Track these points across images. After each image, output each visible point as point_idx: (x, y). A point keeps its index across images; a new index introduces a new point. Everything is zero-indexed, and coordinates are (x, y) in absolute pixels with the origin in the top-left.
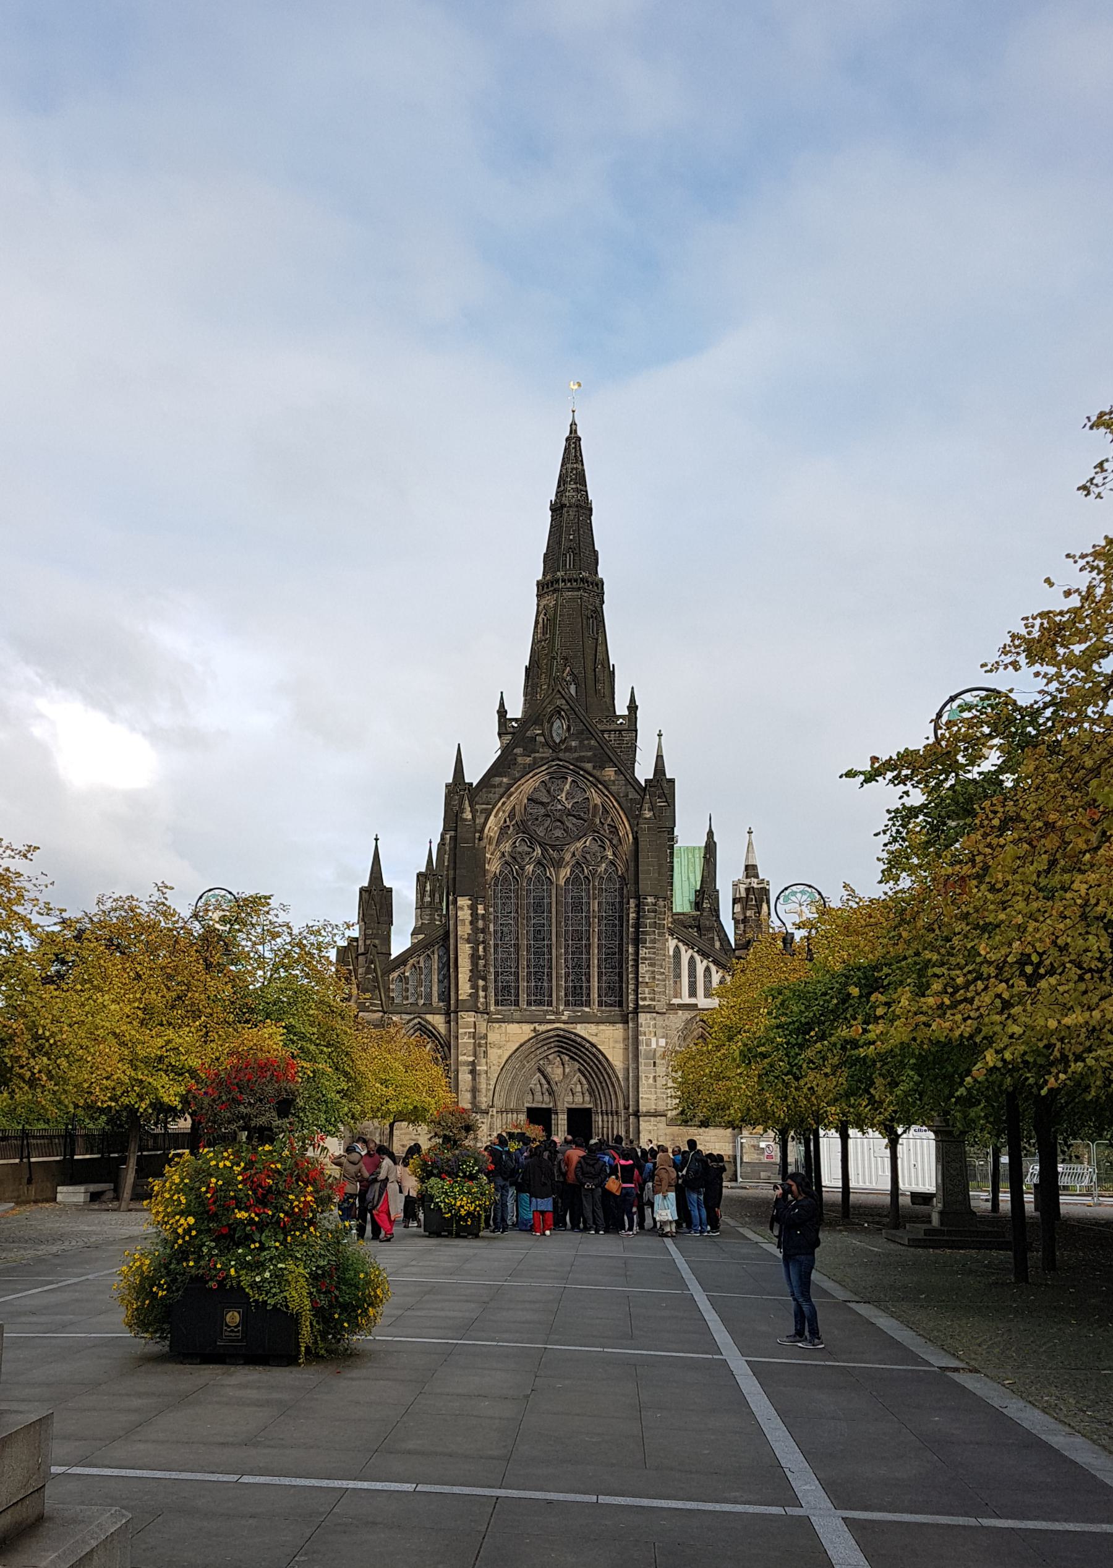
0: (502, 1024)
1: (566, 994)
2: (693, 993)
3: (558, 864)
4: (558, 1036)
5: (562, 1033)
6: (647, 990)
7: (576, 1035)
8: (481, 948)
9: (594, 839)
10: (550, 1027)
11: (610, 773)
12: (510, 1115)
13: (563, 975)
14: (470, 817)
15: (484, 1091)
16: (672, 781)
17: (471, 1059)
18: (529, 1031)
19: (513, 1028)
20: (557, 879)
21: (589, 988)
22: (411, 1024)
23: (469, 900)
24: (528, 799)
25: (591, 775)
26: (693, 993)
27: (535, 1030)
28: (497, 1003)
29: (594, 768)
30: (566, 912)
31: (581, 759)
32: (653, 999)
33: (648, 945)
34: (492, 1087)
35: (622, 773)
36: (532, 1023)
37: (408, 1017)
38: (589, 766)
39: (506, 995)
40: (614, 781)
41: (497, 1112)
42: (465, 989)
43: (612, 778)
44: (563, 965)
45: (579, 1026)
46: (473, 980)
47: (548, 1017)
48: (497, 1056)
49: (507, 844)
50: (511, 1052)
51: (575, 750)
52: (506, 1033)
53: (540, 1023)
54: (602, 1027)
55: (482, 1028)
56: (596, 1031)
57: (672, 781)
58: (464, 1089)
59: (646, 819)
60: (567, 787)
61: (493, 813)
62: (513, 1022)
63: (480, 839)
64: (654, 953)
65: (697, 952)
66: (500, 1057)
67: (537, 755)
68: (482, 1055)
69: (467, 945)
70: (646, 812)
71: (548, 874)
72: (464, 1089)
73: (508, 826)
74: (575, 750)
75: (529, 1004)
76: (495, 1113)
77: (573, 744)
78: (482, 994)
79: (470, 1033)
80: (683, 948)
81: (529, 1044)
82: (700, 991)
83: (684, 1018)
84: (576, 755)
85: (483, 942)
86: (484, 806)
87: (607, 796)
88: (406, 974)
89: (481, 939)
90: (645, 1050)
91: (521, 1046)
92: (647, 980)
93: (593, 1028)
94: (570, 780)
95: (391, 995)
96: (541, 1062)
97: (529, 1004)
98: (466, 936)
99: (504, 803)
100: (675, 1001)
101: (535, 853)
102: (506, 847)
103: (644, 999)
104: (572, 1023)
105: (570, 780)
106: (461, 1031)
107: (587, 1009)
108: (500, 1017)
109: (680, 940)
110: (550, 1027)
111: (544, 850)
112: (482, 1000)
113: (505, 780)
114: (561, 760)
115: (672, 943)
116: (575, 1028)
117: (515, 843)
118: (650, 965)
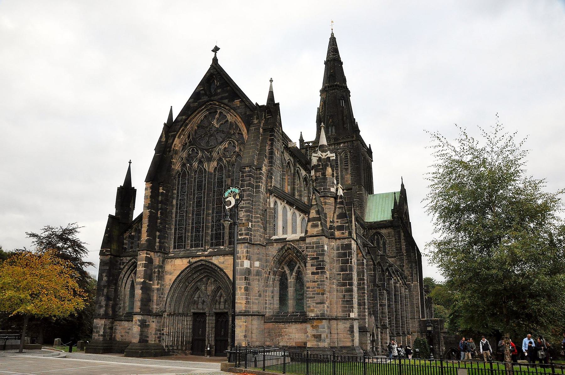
0: (173, 260)
1: (211, 238)
2: (285, 231)
3: (209, 160)
4: (202, 264)
5: (203, 263)
6: (243, 228)
7: (212, 263)
8: (159, 213)
9: (230, 143)
10: (197, 259)
11: (237, 102)
12: (177, 317)
13: (210, 227)
14: (164, 140)
15: (155, 301)
16: (278, 104)
17: (142, 280)
18: (186, 263)
19: (178, 262)
20: (209, 168)
21: (224, 233)
22: (130, 263)
23: (151, 183)
24: (198, 127)
25: (227, 105)
26: (285, 231)
27: (189, 262)
28: (174, 248)
29: (229, 101)
30: (214, 188)
31: (222, 98)
32: (247, 234)
33: (245, 198)
34: (165, 299)
35: (243, 101)
36: (188, 257)
37: (129, 258)
38: (226, 101)
39: (180, 243)
40: (239, 107)
41: (167, 315)
42: (144, 237)
43: (238, 105)
44: (210, 221)
45: (214, 258)
46: (151, 232)
47: (198, 253)
48: (169, 279)
49: (185, 153)
50: (176, 276)
51: (219, 94)
52: (174, 265)
53: (193, 257)
54: (227, 257)
55: (157, 261)
56: (223, 260)
57: (278, 104)
58: (137, 300)
59: (255, 124)
60: (217, 116)
61: (177, 137)
62: (178, 258)
63: (170, 151)
64: (249, 203)
65: (287, 203)
66: (170, 280)
67: (200, 101)
68: (155, 279)
69: (148, 210)
70: (255, 120)
71: (205, 166)
72: (137, 300)
73: (186, 144)
74: (219, 94)
75: (191, 247)
76: (166, 316)
77: (219, 91)
78: (158, 240)
79: (143, 264)
80: (279, 202)
81: (186, 271)
82: (289, 229)
83: (277, 248)
84: (219, 97)
85: (161, 209)
86: (173, 133)
87: (235, 116)
88: (132, 234)
89: (160, 207)
90: (240, 269)
91: (182, 272)
92: (244, 222)
93: (221, 259)
94: (218, 112)
95: (125, 246)
96: (199, 284)
97: (191, 247)
98: (147, 205)
99: (183, 130)
100: (274, 237)
101: (199, 156)
102: (185, 155)
103: (241, 235)
104: (210, 256)
105: (218, 112)
106: (139, 263)
107: (222, 247)
108: (173, 255)
109: (277, 197)
110: (197, 259)
111: (203, 152)
112: (157, 244)
113: (184, 117)
114: (213, 101)
115: (272, 200)
116: (212, 259)
117: (189, 151)
118: (246, 211)
